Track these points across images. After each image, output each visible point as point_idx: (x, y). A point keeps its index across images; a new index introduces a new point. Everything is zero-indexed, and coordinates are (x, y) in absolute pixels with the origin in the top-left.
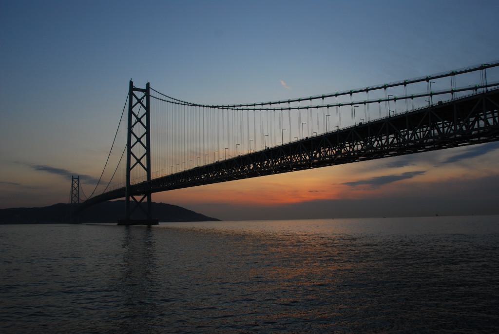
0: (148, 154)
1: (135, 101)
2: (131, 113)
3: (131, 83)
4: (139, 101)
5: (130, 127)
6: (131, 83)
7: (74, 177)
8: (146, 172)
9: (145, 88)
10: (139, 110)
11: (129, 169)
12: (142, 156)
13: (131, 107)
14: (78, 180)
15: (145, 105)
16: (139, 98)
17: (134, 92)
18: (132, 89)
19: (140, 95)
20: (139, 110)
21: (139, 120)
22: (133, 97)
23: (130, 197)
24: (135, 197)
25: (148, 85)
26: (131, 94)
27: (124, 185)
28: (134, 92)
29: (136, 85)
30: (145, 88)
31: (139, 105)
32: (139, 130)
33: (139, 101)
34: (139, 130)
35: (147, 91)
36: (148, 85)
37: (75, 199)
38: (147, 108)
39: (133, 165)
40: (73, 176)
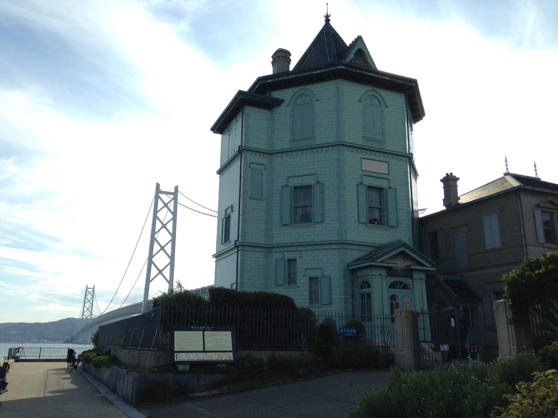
0: (172, 264)
1: (160, 205)
2: (155, 217)
3: (158, 185)
4: (166, 205)
5: (153, 233)
6: (158, 185)
7: (88, 287)
9: (173, 191)
10: (165, 215)
11: (148, 281)
12: (164, 266)
13: (156, 211)
14: (94, 290)
15: (172, 210)
17: (160, 195)
19: (166, 198)
20: (165, 215)
21: (164, 226)
22: (159, 200)
25: (176, 188)
26: (157, 197)
27: (141, 300)
28: (160, 195)
29: (162, 188)
30: (173, 191)
31: (165, 209)
32: (163, 237)
33: (166, 205)
34: (163, 237)
35: (175, 194)
36: (176, 188)
37: (87, 314)
38: (175, 213)
39: (153, 277)
40: (87, 286)
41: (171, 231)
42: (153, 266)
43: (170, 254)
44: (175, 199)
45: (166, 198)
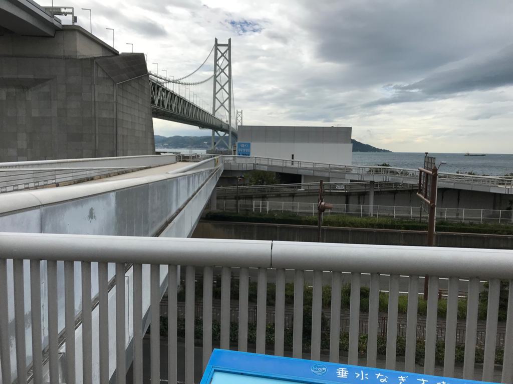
1: (219, 55)
3: (216, 40)
6: (216, 40)
8: (228, 113)
9: (227, 43)
10: (222, 62)
16: (223, 52)
18: (217, 45)
20: (222, 62)
23: (215, 132)
24: (219, 132)
25: (230, 40)
26: (216, 50)
29: (218, 43)
30: (227, 43)
33: (223, 55)
35: (229, 46)
36: (230, 40)
41: (228, 75)
42: (216, 99)
43: (228, 92)
44: (229, 49)
45: (223, 49)
